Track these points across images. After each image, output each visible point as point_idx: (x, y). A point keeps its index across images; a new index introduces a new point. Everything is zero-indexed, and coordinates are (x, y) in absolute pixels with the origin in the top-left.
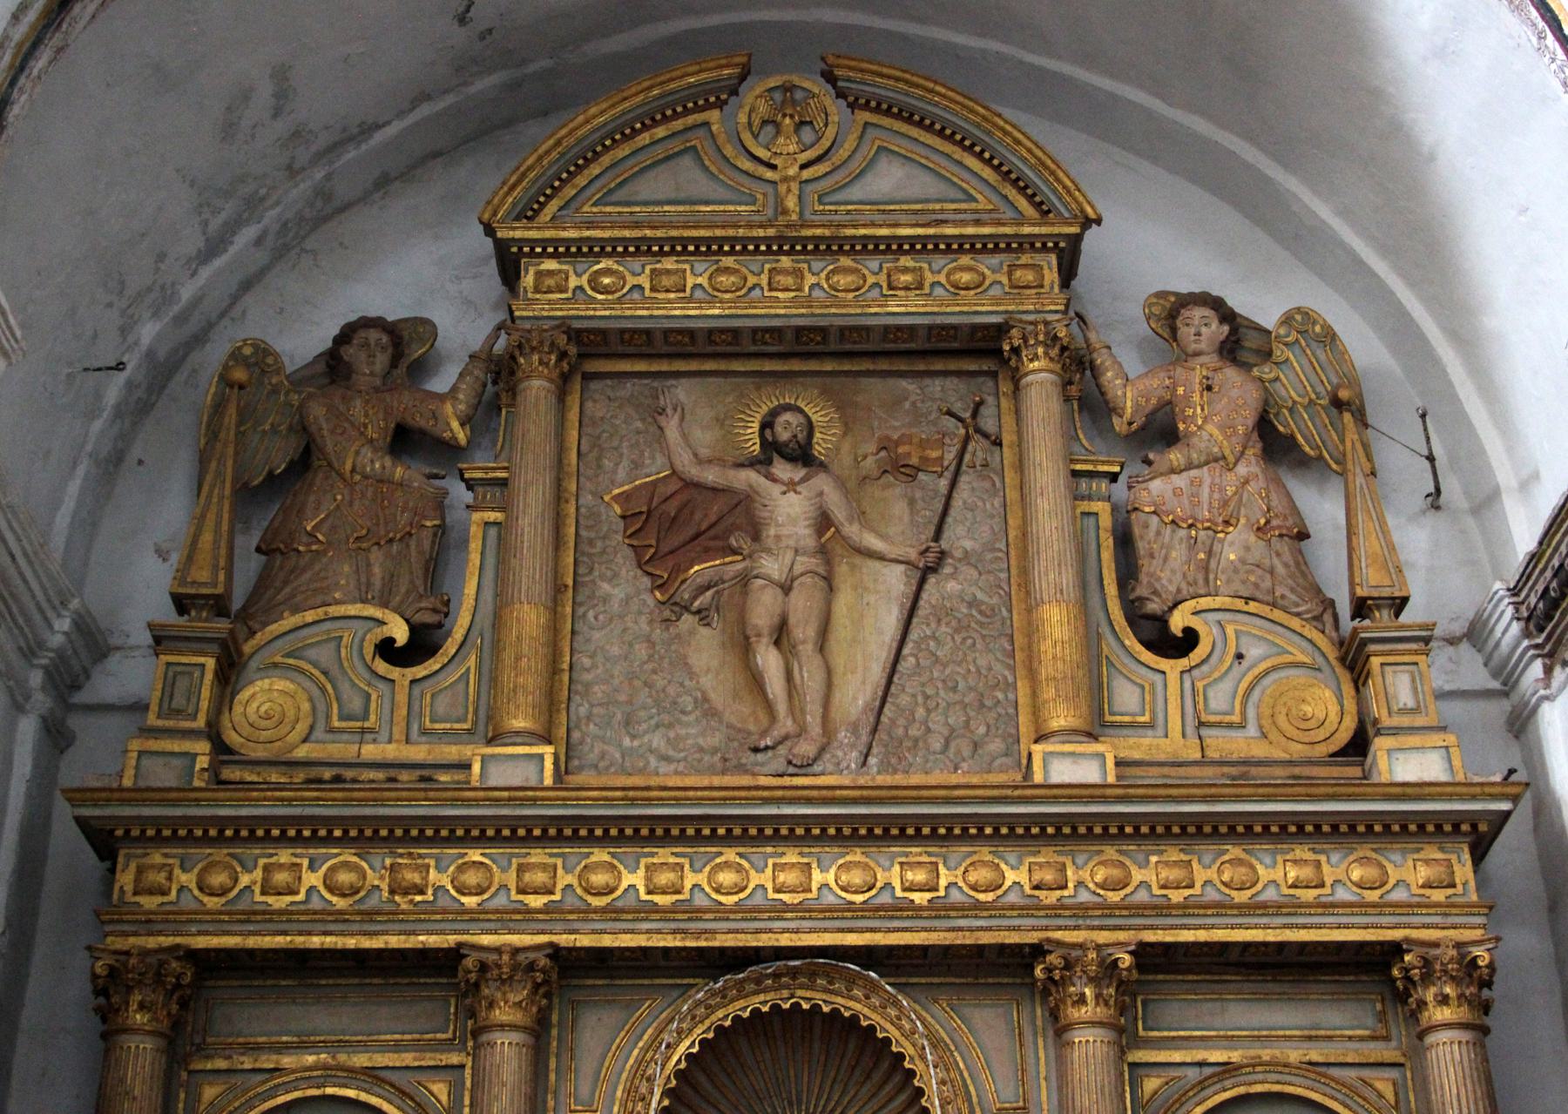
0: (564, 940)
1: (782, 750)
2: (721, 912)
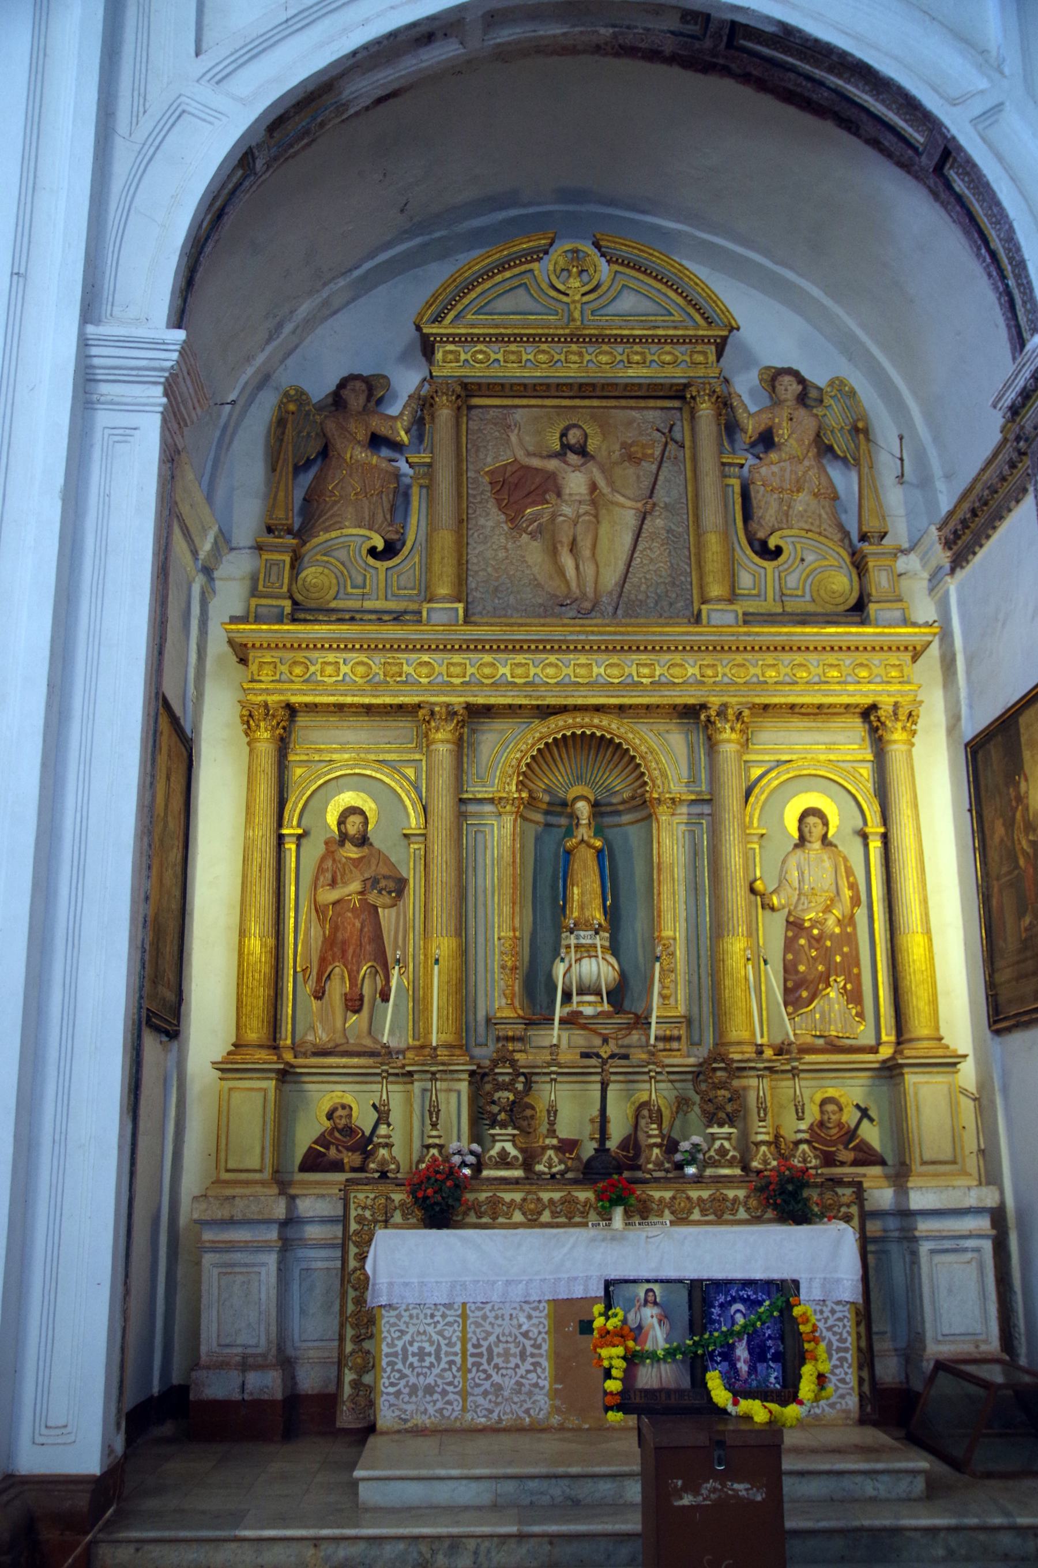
0: (471, 700)
1: (574, 606)
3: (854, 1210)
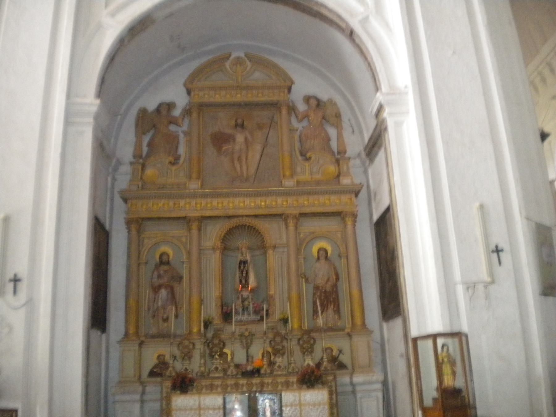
3: (333, 384)
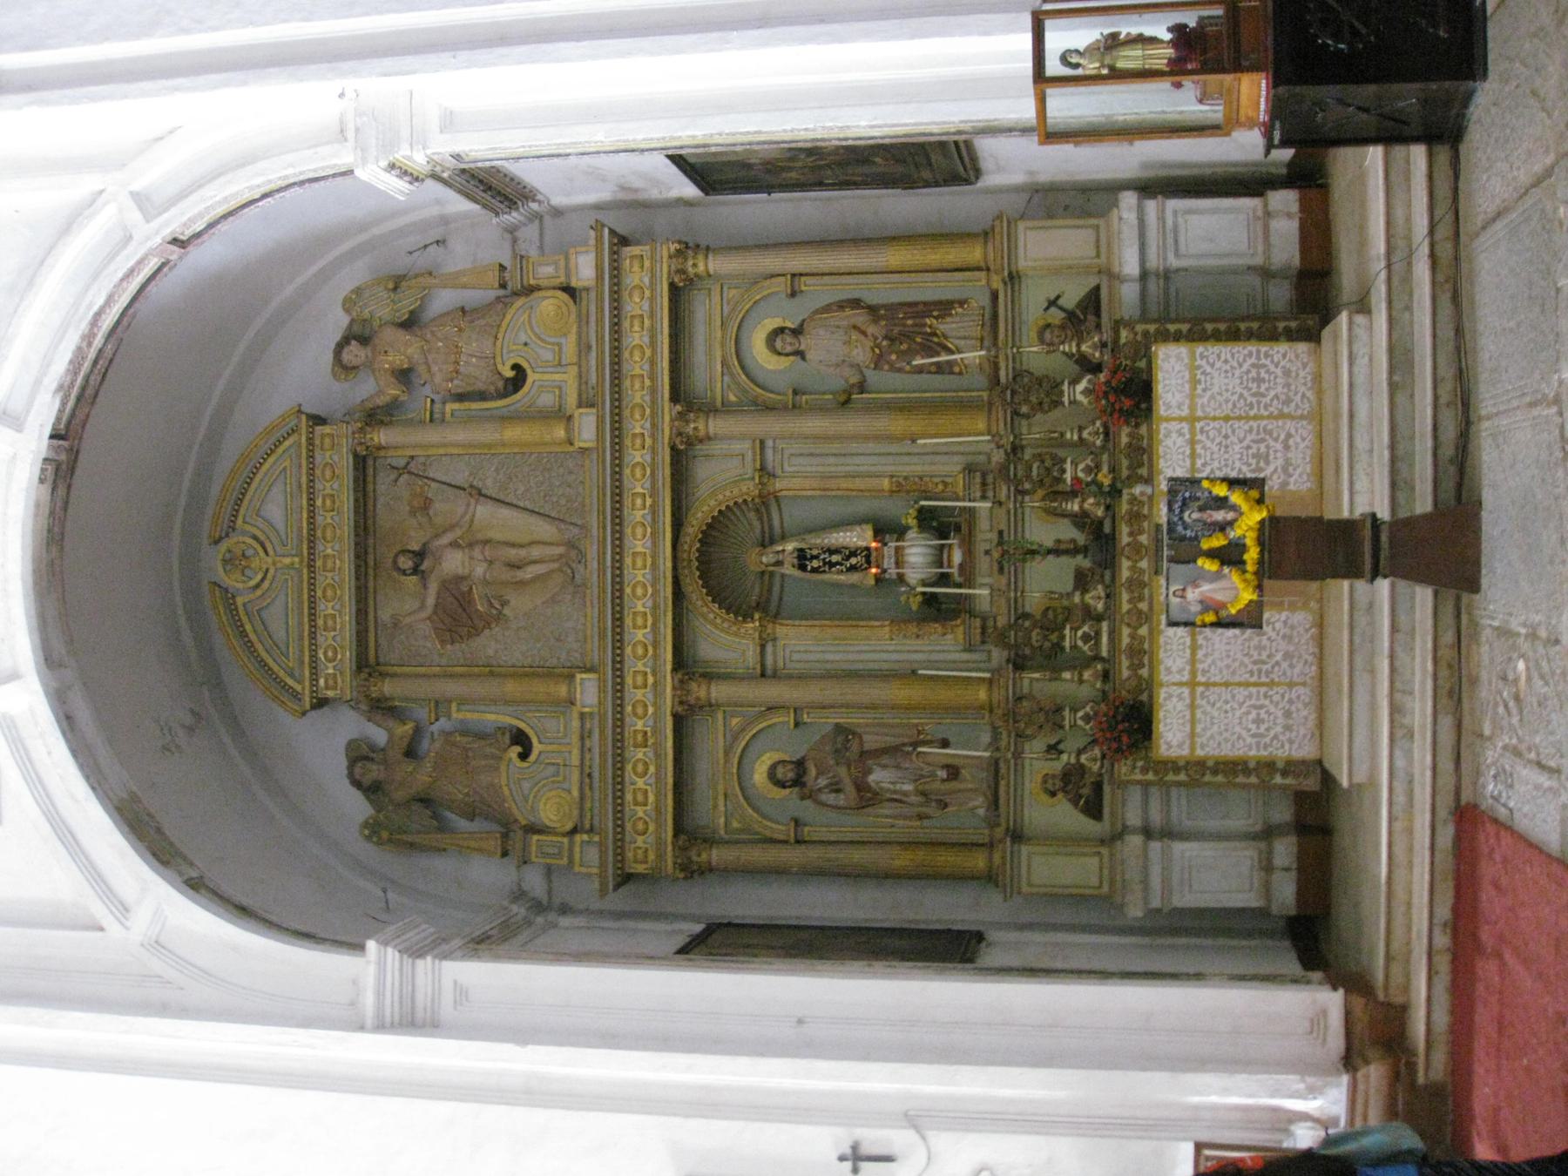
0: (669, 667)
1: (574, 565)
2: (655, 593)
3: (1139, 328)
